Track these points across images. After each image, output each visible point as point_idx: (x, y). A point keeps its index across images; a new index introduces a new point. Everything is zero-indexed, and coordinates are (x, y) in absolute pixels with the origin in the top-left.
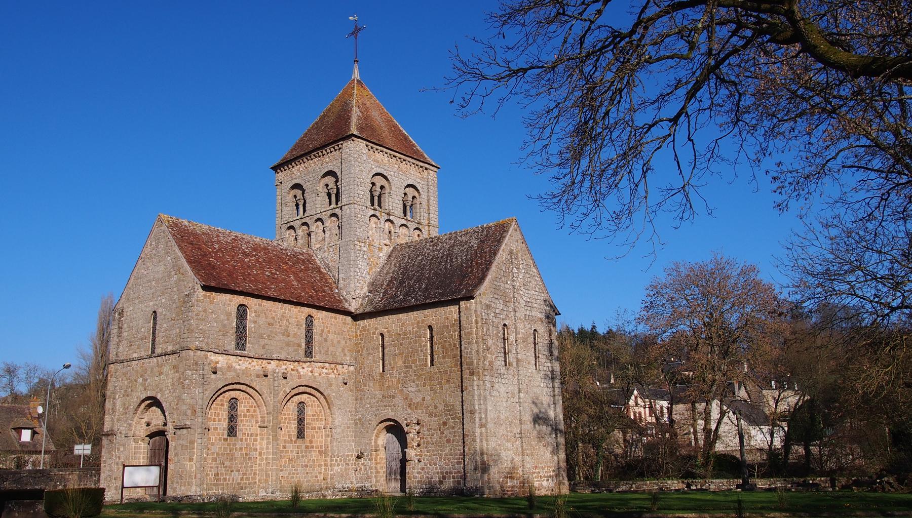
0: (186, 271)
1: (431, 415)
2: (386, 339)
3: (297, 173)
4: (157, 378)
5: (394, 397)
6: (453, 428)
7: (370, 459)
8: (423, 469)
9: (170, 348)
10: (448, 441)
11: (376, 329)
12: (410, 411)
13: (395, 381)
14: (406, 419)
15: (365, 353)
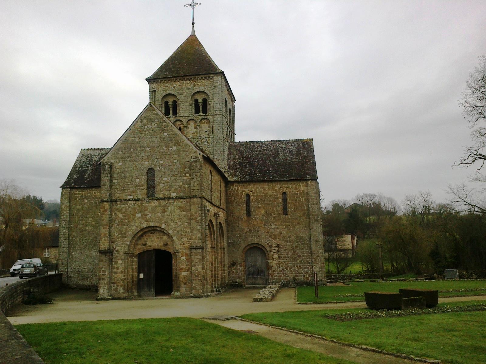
0: (187, 145)
1: (286, 241)
2: (252, 198)
3: (171, 87)
4: (160, 215)
5: (258, 231)
6: (303, 249)
7: (240, 266)
8: (281, 271)
9: (173, 195)
10: (299, 256)
11: (243, 191)
12: (271, 239)
13: (259, 222)
14: (268, 244)
15: (234, 204)
